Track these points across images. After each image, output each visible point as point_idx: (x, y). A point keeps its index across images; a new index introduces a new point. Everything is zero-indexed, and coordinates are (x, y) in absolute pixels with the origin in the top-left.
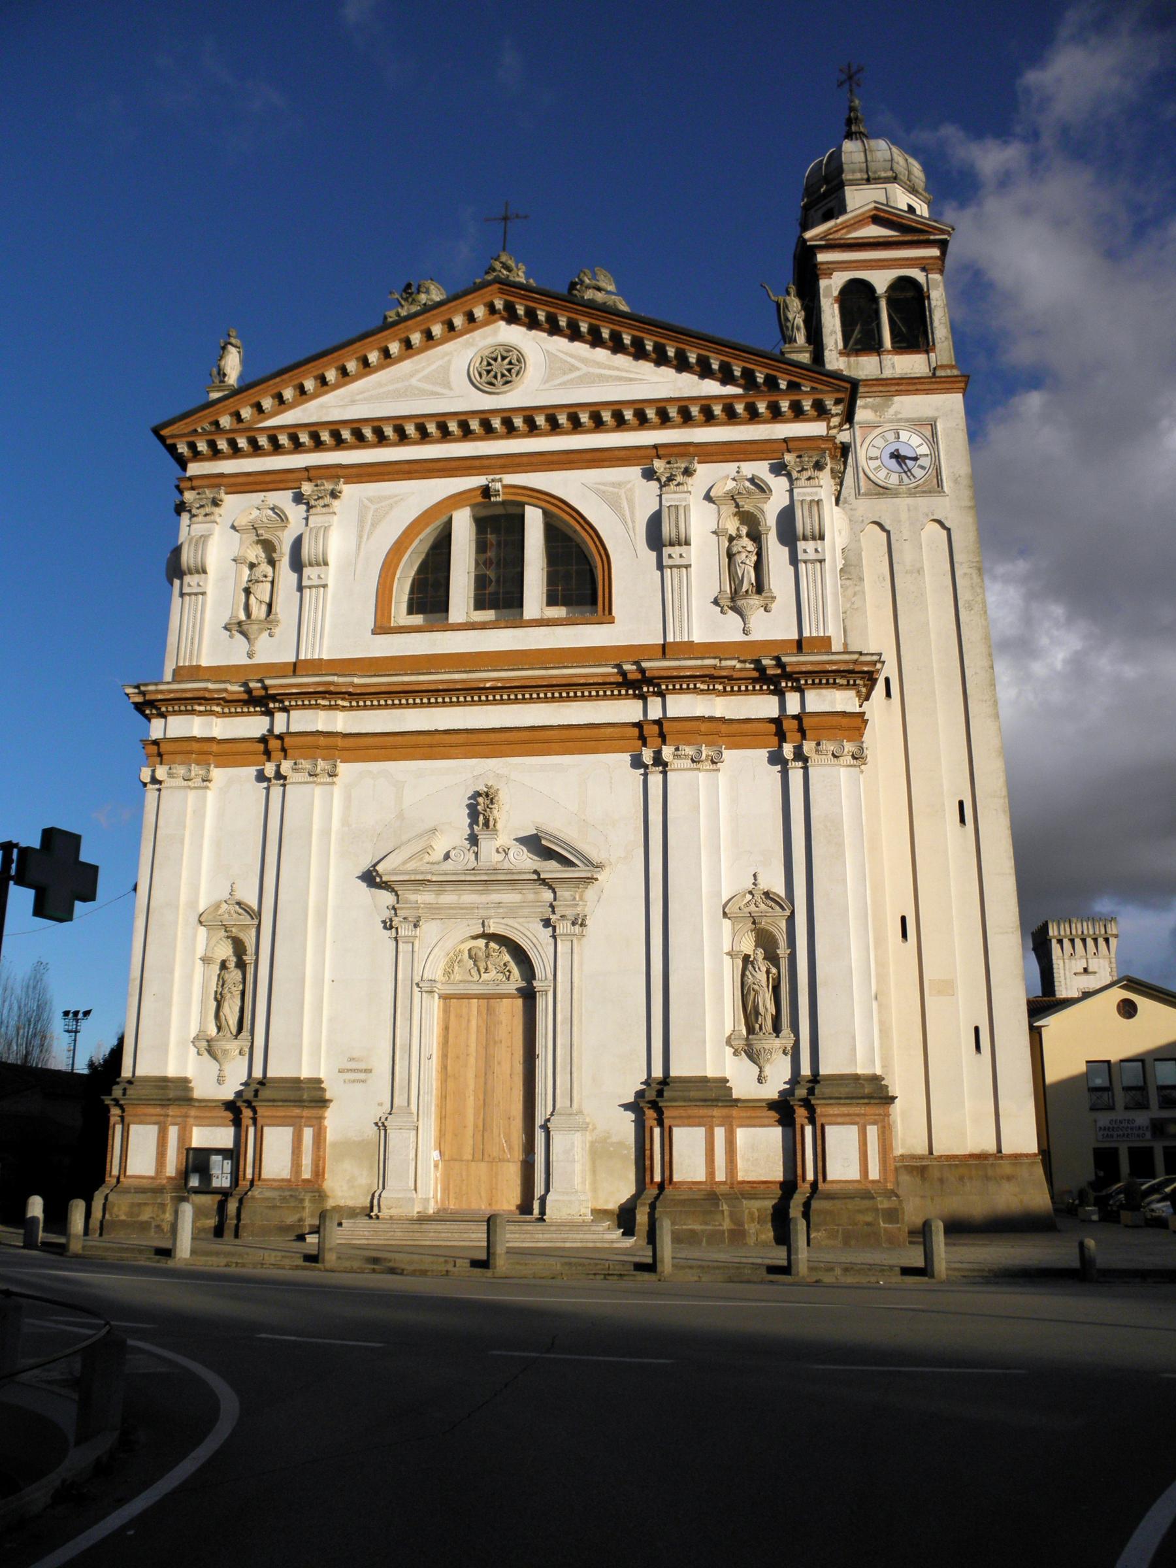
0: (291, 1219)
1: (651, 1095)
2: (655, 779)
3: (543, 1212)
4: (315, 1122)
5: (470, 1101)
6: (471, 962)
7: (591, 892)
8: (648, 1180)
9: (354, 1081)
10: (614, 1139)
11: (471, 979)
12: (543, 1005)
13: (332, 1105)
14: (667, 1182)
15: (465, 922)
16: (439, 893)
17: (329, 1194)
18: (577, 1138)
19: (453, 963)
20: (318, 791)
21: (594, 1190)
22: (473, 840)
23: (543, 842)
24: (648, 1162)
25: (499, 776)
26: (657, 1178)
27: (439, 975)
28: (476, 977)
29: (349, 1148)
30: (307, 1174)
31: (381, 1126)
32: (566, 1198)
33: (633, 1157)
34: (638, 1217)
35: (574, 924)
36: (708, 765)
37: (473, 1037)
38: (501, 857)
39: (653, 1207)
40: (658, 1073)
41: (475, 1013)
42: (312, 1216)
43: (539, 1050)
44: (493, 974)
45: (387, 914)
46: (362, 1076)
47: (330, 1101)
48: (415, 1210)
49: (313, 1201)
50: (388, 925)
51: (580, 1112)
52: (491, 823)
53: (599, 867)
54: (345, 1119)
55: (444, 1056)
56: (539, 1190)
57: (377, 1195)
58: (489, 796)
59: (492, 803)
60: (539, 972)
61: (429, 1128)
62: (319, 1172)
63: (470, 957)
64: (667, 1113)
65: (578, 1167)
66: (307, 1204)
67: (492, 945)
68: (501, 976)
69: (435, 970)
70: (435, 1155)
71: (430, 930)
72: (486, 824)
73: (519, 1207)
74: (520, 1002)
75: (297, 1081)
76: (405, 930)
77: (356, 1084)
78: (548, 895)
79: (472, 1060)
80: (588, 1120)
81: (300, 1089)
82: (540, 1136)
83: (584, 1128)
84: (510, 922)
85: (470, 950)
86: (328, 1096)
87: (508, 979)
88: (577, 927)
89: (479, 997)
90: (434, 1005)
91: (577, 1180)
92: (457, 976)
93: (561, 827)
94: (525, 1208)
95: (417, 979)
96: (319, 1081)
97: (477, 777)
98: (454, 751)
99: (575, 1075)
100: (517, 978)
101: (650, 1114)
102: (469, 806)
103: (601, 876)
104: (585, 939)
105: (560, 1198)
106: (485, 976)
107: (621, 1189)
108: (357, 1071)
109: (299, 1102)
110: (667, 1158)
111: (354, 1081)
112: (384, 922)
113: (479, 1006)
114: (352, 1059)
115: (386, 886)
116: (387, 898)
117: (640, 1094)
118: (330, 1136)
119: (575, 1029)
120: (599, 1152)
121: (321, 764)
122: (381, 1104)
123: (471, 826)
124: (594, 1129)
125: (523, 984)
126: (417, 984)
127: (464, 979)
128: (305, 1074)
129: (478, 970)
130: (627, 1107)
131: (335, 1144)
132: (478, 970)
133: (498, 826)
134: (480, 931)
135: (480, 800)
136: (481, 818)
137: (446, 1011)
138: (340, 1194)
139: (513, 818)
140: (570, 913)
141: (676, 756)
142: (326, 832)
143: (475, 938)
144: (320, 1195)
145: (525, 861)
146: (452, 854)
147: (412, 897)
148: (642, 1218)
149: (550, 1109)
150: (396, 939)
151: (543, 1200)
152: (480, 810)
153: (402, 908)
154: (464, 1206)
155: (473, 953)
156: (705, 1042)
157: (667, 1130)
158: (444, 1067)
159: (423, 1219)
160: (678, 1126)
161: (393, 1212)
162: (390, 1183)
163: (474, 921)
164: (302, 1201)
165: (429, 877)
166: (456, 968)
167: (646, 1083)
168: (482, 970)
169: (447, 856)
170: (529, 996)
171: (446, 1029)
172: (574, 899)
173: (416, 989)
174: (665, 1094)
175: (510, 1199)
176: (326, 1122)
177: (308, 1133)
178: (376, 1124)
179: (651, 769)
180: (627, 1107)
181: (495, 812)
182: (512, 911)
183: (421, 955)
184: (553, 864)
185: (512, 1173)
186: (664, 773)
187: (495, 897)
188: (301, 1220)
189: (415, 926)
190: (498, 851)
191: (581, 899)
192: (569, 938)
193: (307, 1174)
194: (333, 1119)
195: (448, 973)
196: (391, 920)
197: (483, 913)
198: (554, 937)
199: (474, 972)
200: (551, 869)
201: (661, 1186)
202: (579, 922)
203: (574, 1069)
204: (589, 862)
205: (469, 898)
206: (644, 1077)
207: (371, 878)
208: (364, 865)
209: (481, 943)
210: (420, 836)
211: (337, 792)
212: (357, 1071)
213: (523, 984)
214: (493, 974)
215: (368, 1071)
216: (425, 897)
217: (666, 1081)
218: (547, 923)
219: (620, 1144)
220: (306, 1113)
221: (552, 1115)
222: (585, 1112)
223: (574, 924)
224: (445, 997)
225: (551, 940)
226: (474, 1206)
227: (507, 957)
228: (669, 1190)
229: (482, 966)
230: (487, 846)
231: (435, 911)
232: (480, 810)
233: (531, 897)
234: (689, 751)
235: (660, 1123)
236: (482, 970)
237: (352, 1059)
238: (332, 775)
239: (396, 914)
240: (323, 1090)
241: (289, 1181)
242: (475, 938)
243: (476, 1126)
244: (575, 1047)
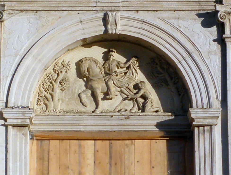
6: (81, 83)
11: (83, 109)
15: (75, 17)
19: (53, 81)
27: (31, 100)
28: (91, 106)
41: (91, 161)
44: (117, 101)
60: (197, 95)
63: (80, 74)
67: (116, 56)
68: (129, 104)
85: (79, 64)
87: (143, 109)
89: (95, 137)
92: (61, 102)
100: (156, 112)
106: (104, 105)
113: (96, 152)
125: (168, 117)
127: (69, 108)
129: (94, 95)
132: (94, 95)
134: (100, 30)
137: (43, 159)
143: (87, 43)
155: (85, 68)
166: (58, 90)
168: (100, 96)
195: (45, 98)
199: (87, 98)
209: (97, 52)
213: (168, 117)
214: (117, 101)
224: (42, 138)
225: (216, 48)
227: (140, 76)
229: (100, 87)
236: (100, 96)
242: (87, 43)
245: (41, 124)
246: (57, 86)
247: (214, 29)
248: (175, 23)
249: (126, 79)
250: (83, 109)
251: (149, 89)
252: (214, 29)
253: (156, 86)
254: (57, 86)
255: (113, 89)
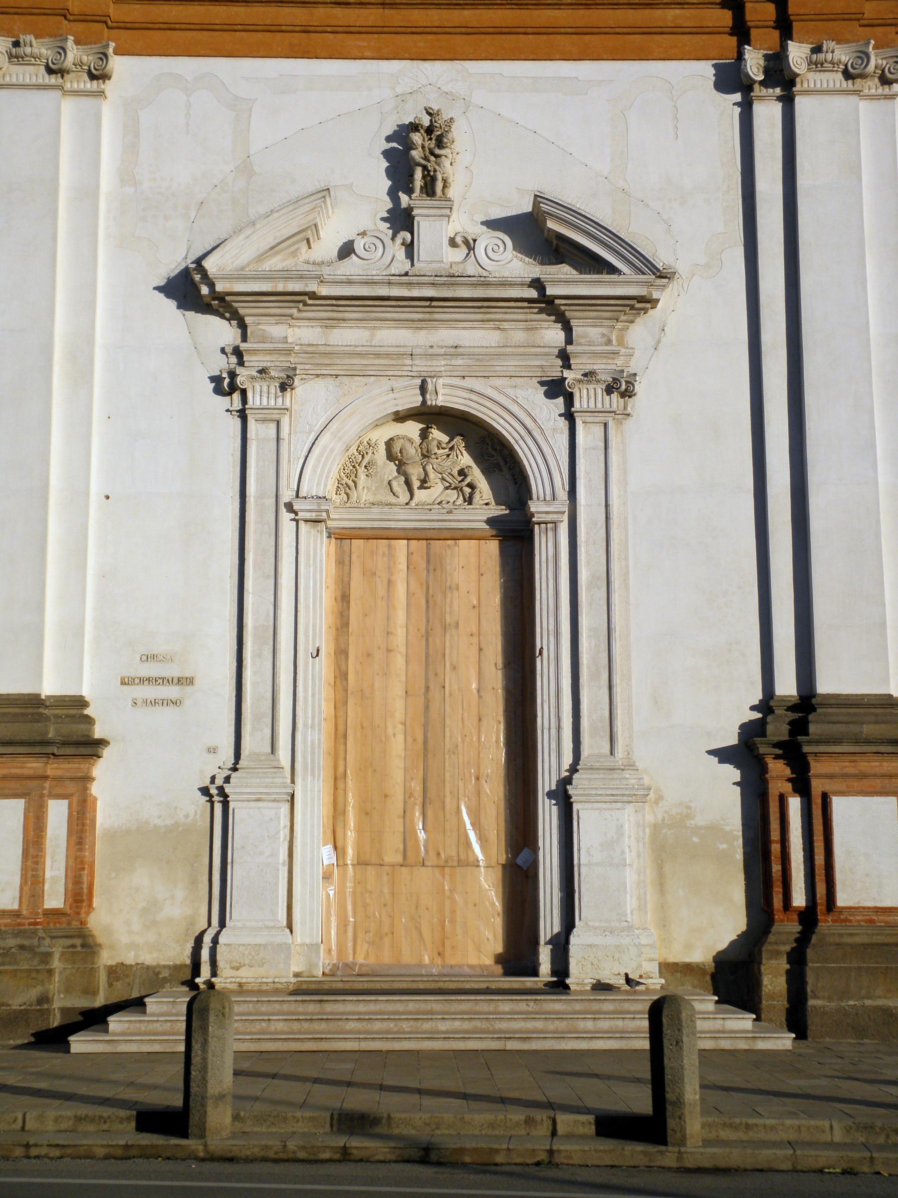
0: (21, 998)
1: (778, 730)
2: (768, 113)
3: (561, 969)
4: (71, 787)
5: (397, 745)
6: (392, 467)
7: (640, 332)
8: (777, 901)
9: (155, 703)
10: (700, 820)
11: (393, 500)
12: (549, 550)
13: (106, 752)
14: (821, 908)
15: (385, 384)
16: (330, 324)
17: (100, 939)
18: (628, 816)
20: (68, 107)
21: (663, 924)
22: (401, 220)
23: (551, 224)
24: (776, 868)
25: (452, 97)
26: (799, 899)
27: (329, 488)
28: (404, 496)
29: (143, 842)
30: (54, 898)
31: (217, 795)
32: (610, 940)
33: (739, 856)
34: (766, 981)
35: (609, 390)
36: (872, 86)
37: (401, 616)
38: (459, 254)
39: (797, 960)
40: (787, 686)
41: (403, 566)
42: (68, 989)
43: (543, 638)
44: (437, 490)
45: (221, 364)
46: (171, 692)
47: (102, 743)
48: (292, 967)
49: (70, 955)
50: (226, 385)
51: (631, 766)
52: (439, 185)
53: (664, 275)
54: (141, 779)
55: (341, 653)
56: (549, 923)
57: (207, 939)
58: (436, 134)
59: (440, 143)
61: (313, 794)
62: (80, 894)
63: (390, 457)
64: (816, 767)
65: (630, 877)
66: (56, 963)
67: (436, 434)
68: (453, 495)
69: (322, 479)
70: (327, 854)
71: (312, 398)
72: (429, 189)
73: (500, 959)
74: (493, 546)
75: (34, 701)
76: (260, 396)
77: (158, 708)
78: (554, 335)
79: (399, 661)
80: (647, 781)
81: (39, 718)
82: (547, 816)
83: (639, 796)
84: (478, 385)
85: (389, 444)
86: (98, 733)
87: (469, 500)
88: (615, 396)
89: (409, 536)
90: (318, 549)
91: (630, 903)
92: (366, 490)
93: (584, 190)
94: (518, 957)
95: (287, 495)
96: (80, 702)
97: (402, 98)
98: (351, 41)
99: (618, 689)
100: (486, 505)
101: (778, 771)
102: (387, 154)
103: (666, 297)
104: (629, 423)
105: (599, 940)
106: (421, 495)
107: (717, 921)
108: (161, 682)
109: (40, 746)
110: (820, 859)
111: (155, 703)
112: (216, 380)
113: (409, 554)
114: (149, 658)
115: (220, 305)
116: (222, 331)
117: (751, 733)
118: (104, 817)
119: (616, 599)
120: (669, 847)
121: (73, 53)
122: (212, 750)
123: (393, 193)
124: (660, 798)
126: (289, 507)
127: (377, 498)
128: (50, 687)
129: (408, 483)
130: (723, 755)
131: (112, 835)
132: (408, 483)
133: (451, 193)
134: (417, 401)
135: (417, 138)
136: (418, 173)
137: (343, 562)
138: (124, 939)
139: (483, 181)
140: (604, 368)
141: (815, 65)
142: (88, 193)
143: (400, 417)
144: (85, 945)
145: (510, 265)
146: (359, 246)
147: (276, 330)
148: (773, 980)
149: (567, 759)
150: (243, 415)
151: (561, 945)
152: (413, 161)
153: (255, 352)
154: (387, 958)
155: (396, 448)
156: (883, 624)
157: (817, 802)
158: (341, 675)
159: (306, 990)
160: (843, 793)
161: (247, 975)
162: (237, 913)
163: (405, 382)
164: (46, 957)
165: (313, 287)
166: (362, 476)
167: (767, 705)
168: (416, 484)
169: (347, 251)
170: (516, 536)
171: (344, 598)
172: (609, 342)
173: (286, 516)
174: (812, 728)
175: (481, 938)
176: (95, 789)
177: (57, 812)
178: (205, 791)
179: (758, 91)
180: (723, 755)
181: (446, 163)
182: (482, 364)
183: (295, 447)
184: (565, 270)
185: (488, 889)
186: (788, 101)
187: (445, 336)
188: (44, 999)
189: (283, 387)
190: (453, 243)
191: (621, 342)
192: (601, 418)
193: (54, 898)
194: (112, 785)
195: (346, 487)
196: (233, 375)
197: (421, 366)
198: (569, 416)
199: (399, 486)
200: (563, 280)
201: (808, 918)
202: (621, 387)
203: (616, 680)
204: (645, 265)
205: (392, 336)
206: (757, 696)
207: (189, 290)
208: (172, 262)
209: (413, 429)
210: (297, 202)
211: (109, 112)
212: (161, 682)
214: (437, 490)
215: (186, 681)
216: (302, 333)
217: (807, 702)
218: (555, 388)
219: (713, 829)
220: (54, 768)
221: (573, 769)
222: (640, 765)
223: (609, 390)
224: (341, 536)
225: (563, 424)
226: (408, 958)
227: (466, 460)
228: (825, 924)
229: (415, 473)
230: (432, 232)
231: (327, 363)
232: (413, 161)
233: (518, 336)
234: (842, 54)
235: (802, 786)
236: (416, 484)
237: (149, 658)
238: (98, 75)
239: (241, 363)
240: (89, 720)
241: (16, 914)
242: (400, 417)
243: (408, 795)
244: (617, 635)
245: (340, 519)
246: (361, 471)
247: (561, 400)
248: (511, 392)
249: (448, 463)
250: (393, 500)
251: (477, 475)
252: (561, 400)
253: (486, 472)
254: (361, 471)
255: (432, 475)
